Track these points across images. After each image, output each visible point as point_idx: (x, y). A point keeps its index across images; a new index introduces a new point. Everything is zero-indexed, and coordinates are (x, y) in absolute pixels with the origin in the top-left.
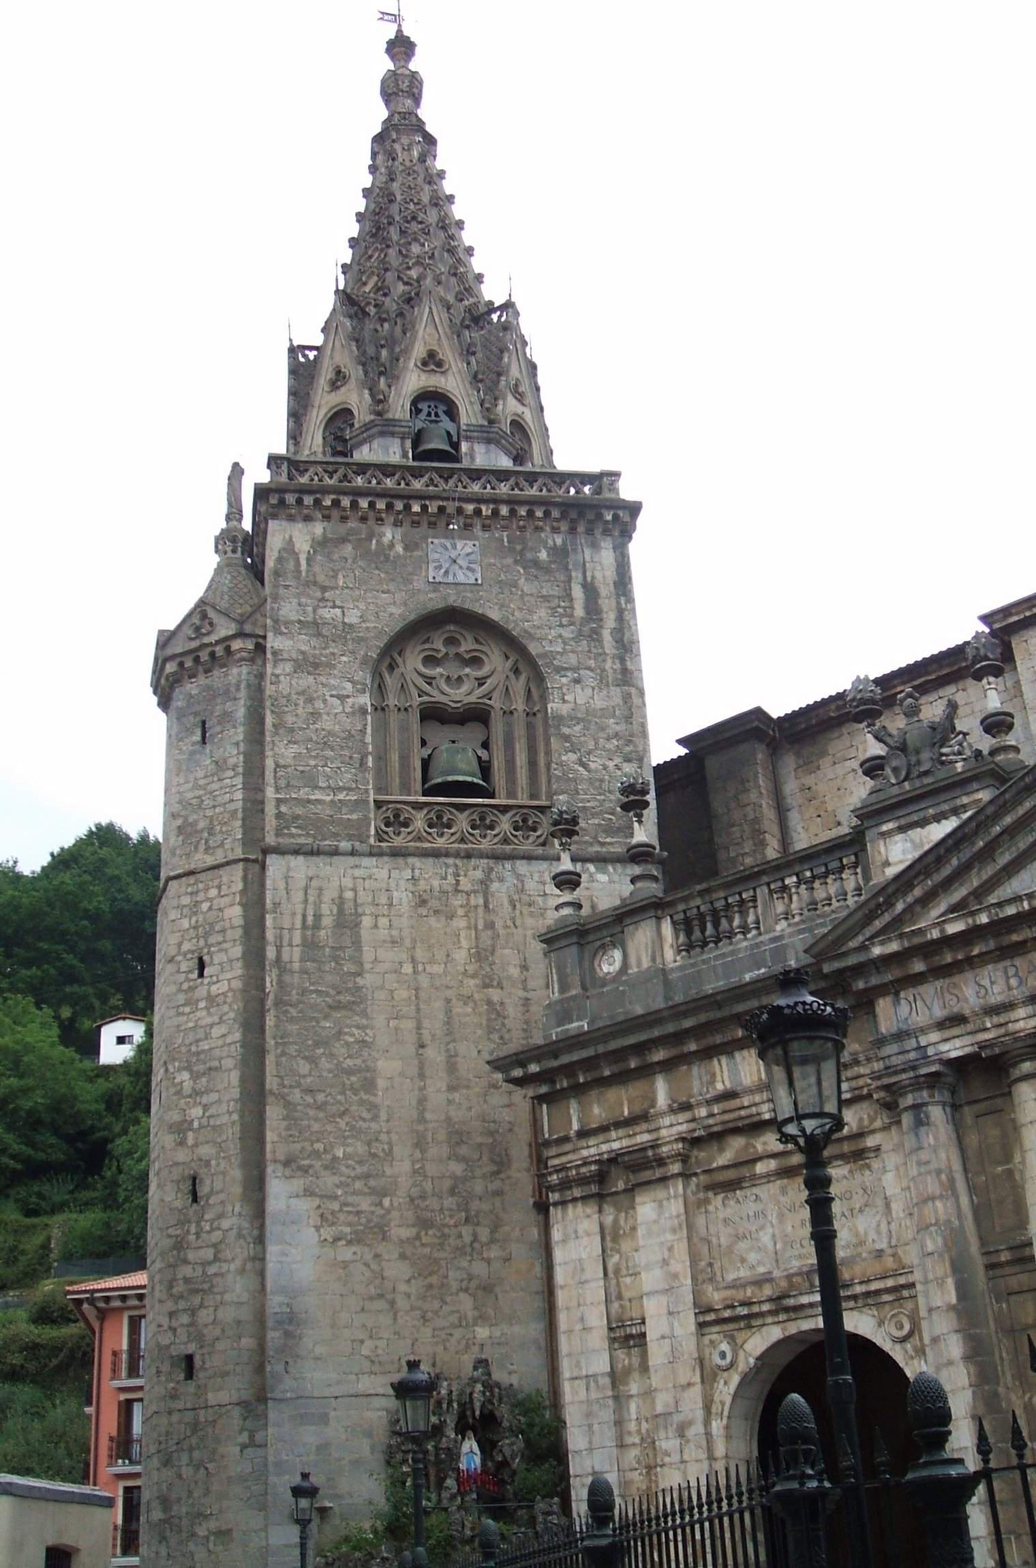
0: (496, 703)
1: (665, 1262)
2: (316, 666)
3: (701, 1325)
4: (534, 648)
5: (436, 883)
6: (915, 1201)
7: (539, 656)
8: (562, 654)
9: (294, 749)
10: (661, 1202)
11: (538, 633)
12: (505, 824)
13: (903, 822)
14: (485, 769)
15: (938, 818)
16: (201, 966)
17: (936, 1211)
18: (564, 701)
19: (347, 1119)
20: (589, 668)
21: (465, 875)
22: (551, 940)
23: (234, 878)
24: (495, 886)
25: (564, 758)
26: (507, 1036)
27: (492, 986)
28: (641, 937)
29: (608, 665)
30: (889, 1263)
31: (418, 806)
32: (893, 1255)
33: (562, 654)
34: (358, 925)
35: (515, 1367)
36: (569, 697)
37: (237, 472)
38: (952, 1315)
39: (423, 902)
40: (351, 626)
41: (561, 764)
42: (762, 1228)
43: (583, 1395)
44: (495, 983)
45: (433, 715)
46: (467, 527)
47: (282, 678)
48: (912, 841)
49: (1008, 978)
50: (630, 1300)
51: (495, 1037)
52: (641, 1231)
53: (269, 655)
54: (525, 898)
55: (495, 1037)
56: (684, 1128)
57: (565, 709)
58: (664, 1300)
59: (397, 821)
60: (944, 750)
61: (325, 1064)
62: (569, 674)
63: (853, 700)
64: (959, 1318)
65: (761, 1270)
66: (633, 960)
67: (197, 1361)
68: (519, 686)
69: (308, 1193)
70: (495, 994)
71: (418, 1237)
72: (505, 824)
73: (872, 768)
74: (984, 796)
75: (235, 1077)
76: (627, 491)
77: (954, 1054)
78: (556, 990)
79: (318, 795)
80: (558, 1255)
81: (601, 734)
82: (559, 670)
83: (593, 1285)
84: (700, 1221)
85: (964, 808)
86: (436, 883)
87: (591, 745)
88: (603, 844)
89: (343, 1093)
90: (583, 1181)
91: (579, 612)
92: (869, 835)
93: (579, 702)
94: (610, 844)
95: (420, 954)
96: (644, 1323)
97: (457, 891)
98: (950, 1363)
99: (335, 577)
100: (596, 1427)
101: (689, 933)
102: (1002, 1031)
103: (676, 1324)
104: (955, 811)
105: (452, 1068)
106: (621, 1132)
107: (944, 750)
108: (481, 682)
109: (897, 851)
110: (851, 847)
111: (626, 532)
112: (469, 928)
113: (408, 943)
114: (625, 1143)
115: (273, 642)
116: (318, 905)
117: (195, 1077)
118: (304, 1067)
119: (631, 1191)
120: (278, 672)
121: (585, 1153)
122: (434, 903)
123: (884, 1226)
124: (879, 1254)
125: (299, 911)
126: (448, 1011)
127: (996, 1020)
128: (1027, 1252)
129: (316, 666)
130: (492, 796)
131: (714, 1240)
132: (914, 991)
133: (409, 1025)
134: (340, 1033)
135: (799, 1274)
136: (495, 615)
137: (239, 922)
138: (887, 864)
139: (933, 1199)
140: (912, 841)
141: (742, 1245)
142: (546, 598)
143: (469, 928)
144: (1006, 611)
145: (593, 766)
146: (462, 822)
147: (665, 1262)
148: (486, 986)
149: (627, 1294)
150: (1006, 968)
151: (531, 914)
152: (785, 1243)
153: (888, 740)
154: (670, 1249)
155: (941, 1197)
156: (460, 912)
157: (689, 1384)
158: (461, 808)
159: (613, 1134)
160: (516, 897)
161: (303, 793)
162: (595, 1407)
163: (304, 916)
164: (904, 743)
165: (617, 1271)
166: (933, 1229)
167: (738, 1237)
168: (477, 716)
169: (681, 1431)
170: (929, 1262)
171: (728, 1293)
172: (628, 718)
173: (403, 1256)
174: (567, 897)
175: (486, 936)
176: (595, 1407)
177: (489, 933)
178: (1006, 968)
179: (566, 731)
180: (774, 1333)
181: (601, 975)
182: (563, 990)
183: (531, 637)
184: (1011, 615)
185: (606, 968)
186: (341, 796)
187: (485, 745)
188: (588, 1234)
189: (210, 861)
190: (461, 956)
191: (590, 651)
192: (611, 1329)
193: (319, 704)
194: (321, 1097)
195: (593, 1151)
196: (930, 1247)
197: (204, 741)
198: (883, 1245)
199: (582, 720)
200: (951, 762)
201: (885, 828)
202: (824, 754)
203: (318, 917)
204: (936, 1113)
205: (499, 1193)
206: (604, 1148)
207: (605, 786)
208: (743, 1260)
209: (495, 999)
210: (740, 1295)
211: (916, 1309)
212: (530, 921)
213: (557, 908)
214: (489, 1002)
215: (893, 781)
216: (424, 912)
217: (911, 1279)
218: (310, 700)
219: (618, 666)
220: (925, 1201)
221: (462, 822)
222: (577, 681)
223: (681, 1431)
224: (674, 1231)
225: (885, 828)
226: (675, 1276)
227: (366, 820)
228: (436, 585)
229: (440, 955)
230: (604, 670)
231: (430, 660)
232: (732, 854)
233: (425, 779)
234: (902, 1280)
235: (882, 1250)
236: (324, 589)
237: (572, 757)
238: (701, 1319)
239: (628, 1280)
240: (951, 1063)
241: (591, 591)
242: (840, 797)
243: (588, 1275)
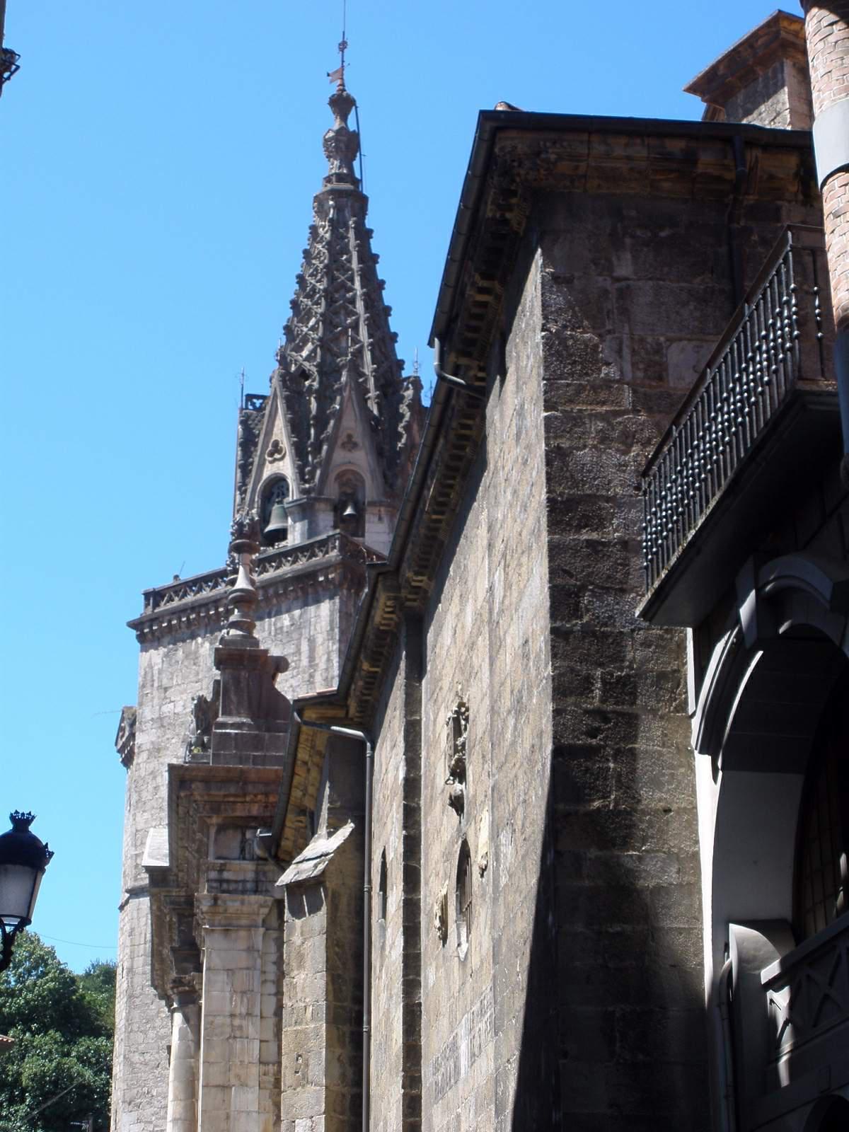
9: (146, 815)
19: (159, 1069)
40: (178, 714)
47: (141, 765)
61: (151, 1034)
69: (139, 1121)
89: (158, 1053)
118: (140, 1037)
120: (139, 761)
125: (143, 932)
129: (159, 750)
134: (159, 1012)
163: (146, 934)
194: (147, 1057)
218: (155, 778)
241: (312, 641)
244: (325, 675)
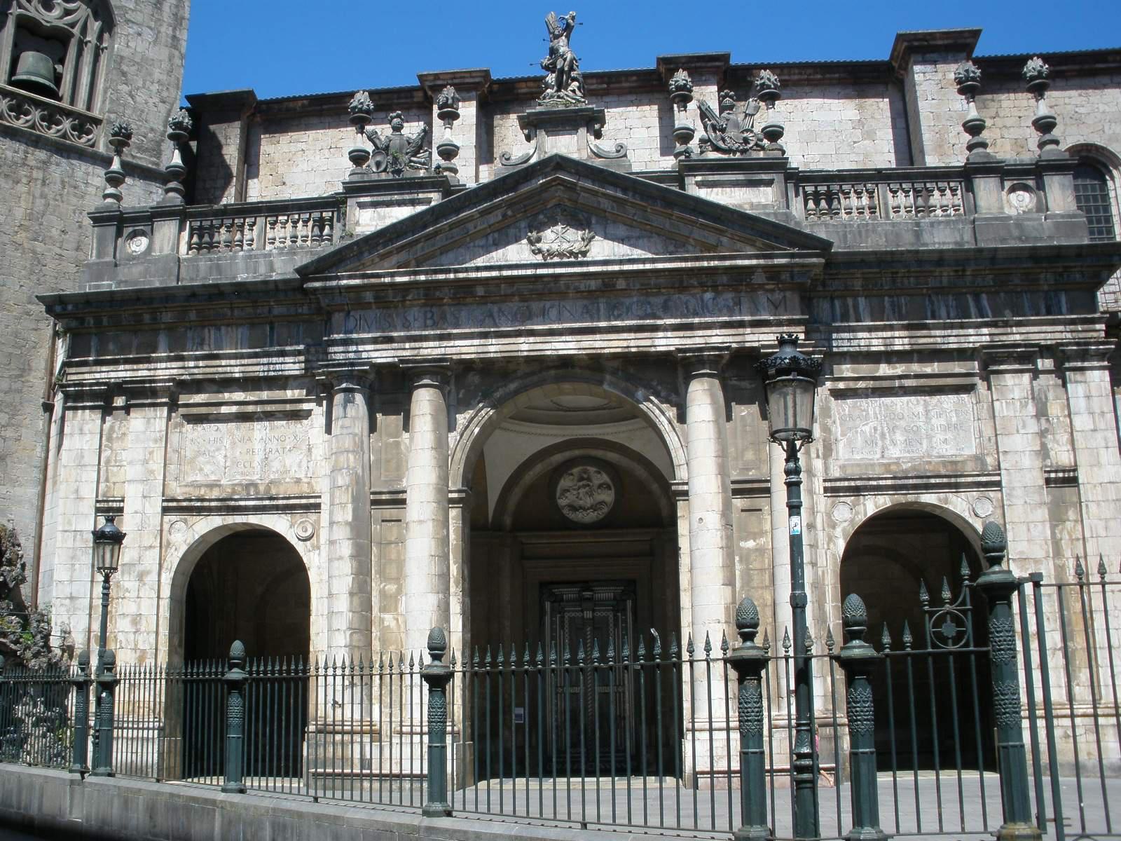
1: (146, 462)
3: (166, 510)
5: (9, 154)
6: (334, 451)
7: (117, 7)
8: (133, 11)
10: (149, 419)
12: (67, 124)
13: (375, 199)
14: (58, 79)
15: (400, 203)
17: (348, 460)
18: (128, 46)
20: (150, 28)
21: (33, 154)
22: (99, 219)
25: (119, 87)
26: (42, 279)
27: (38, 241)
28: (167, 231)
29: (163, 29)
30: (305, 489)
32: (308, 483)
33: (133, 11)
35: (13, 517)
38: (348, 529)
41: (117, 91)
42: (218, 449)
43: (70, 544)
44: (40, 239)
48: (379, 213)
49: (426, 319)
50: (114, 483)
51: (34, 278)
52: (130, 437)
54: (73, 183)
55: (34, 278)
56: (175, 372)
57: (126, 53)
58: (140, 487)
60: (413, 159)
62: (135, 27)
63: (356, 107)
64: (352, 530)
65: (213, 478)
66: (157, 246)
68: (95, 26)
70: (39, 247)
72: (67, 124)
73: (358, 158)
74: (436, 198)
77: (379, 361)
78: (94, 255)
81: (148, 78)
83: (89, 468)
84: (174, 438)
85: (420, 202)
86: (9, 154)
87: (140, 84)
88: (134, 157)
90: (94, 396)
92: (350, 202)
93: (139, 49)
94: (140, 158)
96: (123, 501)
97: (24, 164)
98: (341, 558)
100: (77, 566)
101: (201, 237)
102: (415, 352)
103: (147, 504)
104: (413, 203)
106: (127, 367)
107: (413, 159)
109: (367, 220)
112: (28, 193)
114: (129, 374)
119: (127, 409)
121: (97, 376)
123: (304, 464)
124: (298, 481)
127: (413, 345)
128: (400, 496)
130: (60, 99)
131: (183, 452)
132: (362, 313)
135: (240, 485)
138: (357, 223)
139: (348, 452)
140: (379, 213)
141: (201, 459)
143: (28, 193)
145: (138, 99)
146: (36, 115)
147: (146, 462)
148: (35, 240)
149: (113, 479)
150: (426, 312)
151: (75, 195)
152: (233, 463)
153: (377, 141)
154: (151, 453)
155: (353, 451)
156: (24, 180)
157: (151, 547)
158: (38, 104)
159: (121, 367)
160: (66, 180)
162: (79, 553)
164: (387, 148)
165: (108, 462)
166: (344, 471)
167: (199, 453)
169: (141, 577)
170: (337, 493)
171: (187, 489)
174: (110, 190)
175: (40, 203)
176: (79, 553)
177: (43, 201)
178: (426, 312)
179: (125, 68)
180: (216, 521)
181: (130, 251)
182: (99, 255)
184: (439, 79)
185: (134, 247)
188: (91, 433)
191: (153, 15)
192: (97, 501)
195: (103, 375)
196: (340, 482)
198: (302, 476)
199: (138, 63)
200: (417, 168)
201: (362, 200)
204: (359, 398)
205: (19, 391)
206: (113, 375)
207: (144, 116)
208: (201, 470)
209: (39, 250)
210: (195, 493)
211: (318, 521)
212: (74, 200)
214: (34, 252)
215: (374, 170)
217: (318, 501)
219: (170, 32)
220: (342, 452)
221: (36, 115)
223: (141, 577)
224: (156, 441)
225: (362, 200)
226: (152, 472)
230: (159, 32)
232: (208, 186)
234: (312, 501)
235: (300, 479)
237: (125, 88)
238: (165, 504)
239: (115, 469)
240: (373, 366)
242: (289, 165)
243: (86, 460)
244: (174, 10)
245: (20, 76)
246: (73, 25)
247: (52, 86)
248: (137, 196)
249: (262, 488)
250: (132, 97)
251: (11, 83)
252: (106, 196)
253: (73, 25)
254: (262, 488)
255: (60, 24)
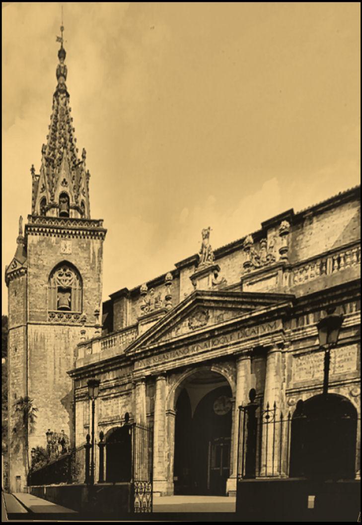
0: (73, 287)
2: (37, 277)
4: (81, 272)
11: (82, 268)
14: (70, 303)
16: (16, 349)
23: (22, 329)
24: (70, 333)
31: (56, 313)
34: (44, 341)
36: (88, 285)
37: (21, 218)
39: (56, 336)
45: (61, 290)
46: (69, 237)
53: (28, 273)
57: (86, 288)
59: (52, 316)
67: (17, 429)
71: (53, 407)
75: (22, 374)
76: (105, 226)
79: (37, 310)
80: (77, 411)
82: (86, 278)
91: (91, 262)
95: (56, 348)
99: (41, 252)
105: (60, 373)
108: (70, 281)
110: (136, 327)
111: (103, 237)
113: (53, 345)
115: (29, 270)
116: (37, 336)
117: (15, 373)
122: (58, 336)
126: (60, 361)
133: (53, 363)
136: (74, 263)
137: (23, 340)
142: (85, 258)
144: (181, 263)
145: (91, 303)
158: (64, 313)
161: (34, 310)
168: (68, 290)
172: (99, 291)
173: (51, 411)
183: (81, 269)
186: (42, 310)
187: (70, 297)
189: (17, 325)
190: (62, 348)
193: (38, 287)
197: (16, 295)
202: (138, 299)
203: (37, 339)
213: (81, 338)
214: (68, 359)
216: (57, 338)
222: (89, 281)
227: (46, 316)
228: (62, 254)
229: (59, 348)
231: (60, 275)
233: (58, 305)
236: (39, 255)
237: (87, 301)
245: (60, 307)
246: (71, 285)
247: (68, 307)
248: (91, 333)
249: (120, 417)
250: (89, 303)
251: (58, 309)
252: (81, 338)
253: (71, 285)
254: (120, 417)
255: (68, 285)
